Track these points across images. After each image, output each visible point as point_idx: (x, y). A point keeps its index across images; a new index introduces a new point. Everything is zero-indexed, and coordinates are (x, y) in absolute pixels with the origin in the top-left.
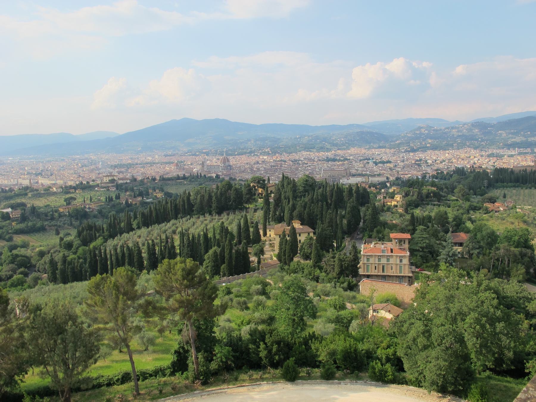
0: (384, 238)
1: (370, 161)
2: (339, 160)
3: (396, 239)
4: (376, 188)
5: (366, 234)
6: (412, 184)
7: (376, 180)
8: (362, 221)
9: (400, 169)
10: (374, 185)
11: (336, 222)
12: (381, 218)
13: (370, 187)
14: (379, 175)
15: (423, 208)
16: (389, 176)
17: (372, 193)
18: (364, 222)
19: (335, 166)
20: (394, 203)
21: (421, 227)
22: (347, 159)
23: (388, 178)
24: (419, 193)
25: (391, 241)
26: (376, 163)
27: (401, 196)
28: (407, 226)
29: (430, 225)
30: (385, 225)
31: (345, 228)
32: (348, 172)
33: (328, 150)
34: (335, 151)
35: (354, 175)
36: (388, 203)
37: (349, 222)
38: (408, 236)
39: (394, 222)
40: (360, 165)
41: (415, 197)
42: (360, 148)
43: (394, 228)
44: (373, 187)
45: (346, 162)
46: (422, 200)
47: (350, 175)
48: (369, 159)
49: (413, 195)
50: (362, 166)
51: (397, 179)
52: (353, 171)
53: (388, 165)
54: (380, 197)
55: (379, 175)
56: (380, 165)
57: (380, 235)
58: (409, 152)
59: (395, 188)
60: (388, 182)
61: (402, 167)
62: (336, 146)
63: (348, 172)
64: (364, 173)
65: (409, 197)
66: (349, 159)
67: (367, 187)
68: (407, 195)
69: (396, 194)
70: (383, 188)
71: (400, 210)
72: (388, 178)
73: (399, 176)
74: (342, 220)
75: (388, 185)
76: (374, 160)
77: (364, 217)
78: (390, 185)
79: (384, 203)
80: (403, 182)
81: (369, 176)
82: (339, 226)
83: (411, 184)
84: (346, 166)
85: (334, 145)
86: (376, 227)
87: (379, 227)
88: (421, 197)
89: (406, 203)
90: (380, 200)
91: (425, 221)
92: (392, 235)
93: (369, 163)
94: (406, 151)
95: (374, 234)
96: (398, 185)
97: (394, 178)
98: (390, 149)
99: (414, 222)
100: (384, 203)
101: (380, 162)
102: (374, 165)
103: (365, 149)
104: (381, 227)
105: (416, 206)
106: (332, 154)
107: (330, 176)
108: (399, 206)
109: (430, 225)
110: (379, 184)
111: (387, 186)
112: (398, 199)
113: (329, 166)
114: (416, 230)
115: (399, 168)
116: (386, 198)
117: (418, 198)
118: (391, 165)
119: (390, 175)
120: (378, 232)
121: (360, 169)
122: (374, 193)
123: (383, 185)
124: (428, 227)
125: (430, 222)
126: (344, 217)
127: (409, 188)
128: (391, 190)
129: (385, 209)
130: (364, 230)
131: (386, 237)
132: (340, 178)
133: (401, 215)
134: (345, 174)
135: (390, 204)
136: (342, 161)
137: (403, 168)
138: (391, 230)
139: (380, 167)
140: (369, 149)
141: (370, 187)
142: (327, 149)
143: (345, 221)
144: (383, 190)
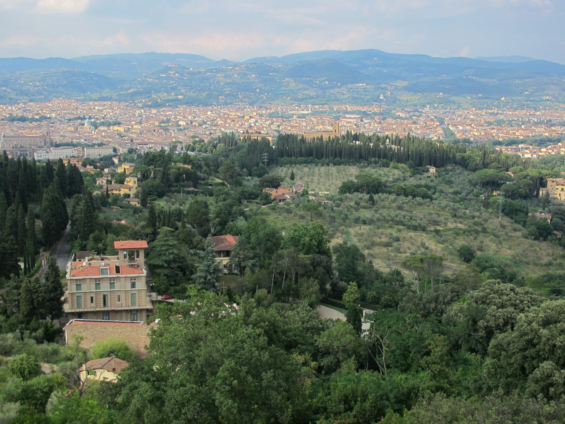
0: (105, 249)
1: (86, 122)
2: (33, 120)
3: (124, 250)
4: (96, 167)
5: (76, 245)
6: (153, 160)
7: (95, 153)
8: (70, 222)
9: (134, 136)
10: (92, 163)
11: (24, 225)
12: (101, 216)
13: (84, 165)
14: (101, 145)
15: (171, 198)
16: (117, 146)
17: (87, 174)
18: (72, 225)
19: (24, 128)
20: (123, 191)
21: (166, 228)
22: (46, 118)
23: (115, 150)
24: (165, 175)
25: (117, 254)
26: (96, 126)
27: (136, 179)
28: (143, 228)
29: (179, 224)
30: (108, 228)
31: (40, 236)
32: (48, 140)
33: (12, 102)
34: (24, 103)
35: (57, 146)
36: (115, 192)
37: (47, 226)
38: (143, 244)
39: (123, 222)
40: (69, 129)
41: (158, 181)
42: (69, 98)
43: (120, 232)
44: (90, 165)
45: (44, 122)
46: (170, 186)
47: (52, 145)
48: (85, 118)
49: (155, 178)
50: (72, 129)
51: (131, 151)
52: (57, 139)
53: (116, 128)
54: (101, 182)
55: (101, 145)
56: (102, 128)
57: (100, 245)
58: (150, 107)
59: (127, 167)
60: (115, 156)
61: (138, 131)
62: (27, 95)
63: (48, 140)
64: (75, 141)
65: (149, 180)
66: (50, 118)
67: (79, 165)
68: (145, 177)
69: (128, 176)
70: (106, 167)
71: (135, 203)
72: (115, 150)
73: (134, 147)
74: (34, 222)
75: (116, 161)
76: (93, 120)
77: (72, 216)
78: (120, 161)
79: (107, 191)
80: (139, 156)
81: (84, 146)
82: (29, 232)
83: (152, 159)
84: (44, 130)
85: (22, 93)
86: (92, 231)
87: (97, 232)
88: (168, 180)
89: (144, 191)
90: (101, 187)
91: (172, 219)
92: (117, 245)
93: (83, 124)
94: (145, 106)
95: (90, 243)
96: (132, 161)
97: (126, 151)
98: (120, 101)
99: (154, 220)
100: (107, 191)
101: (102, 124)
102: (93, 127)
103: (78, 101)
104: (100, 231)
105: (160, 195)
106: (19, 109)
107: (15, 147)
108: (132, 196)
109: (179, 224)
110: (101, 159)
111: (113, 163)
112: (131, 184)
113: (15, 129)
114: (158, 234)
115: (133, 133)
116: (111, 183)
117: (162, 182)
118: (121, 129)
119: (120, 145)
120: (97, 240)
121: (69, 135)
122: (92, 175)
123: (107, 161)
124: (177, 229)
125: (179, 220)
126: (38, 217)
127: (149, 165)
128: (120, 170)
129: (110, 200)
130: (72, 238)
131: (108, 248)
132: (34, 151)
133: (136, 211)
134: (43, 144)
135: (117, 192)
136: (36, 120)
137: (141, 134)
138: (117, 236)
139: (102, 131)
140: (84, 101)
141: (84, 165)
142: (10, 99)
143: (39, 223)
144: (106, 170)
